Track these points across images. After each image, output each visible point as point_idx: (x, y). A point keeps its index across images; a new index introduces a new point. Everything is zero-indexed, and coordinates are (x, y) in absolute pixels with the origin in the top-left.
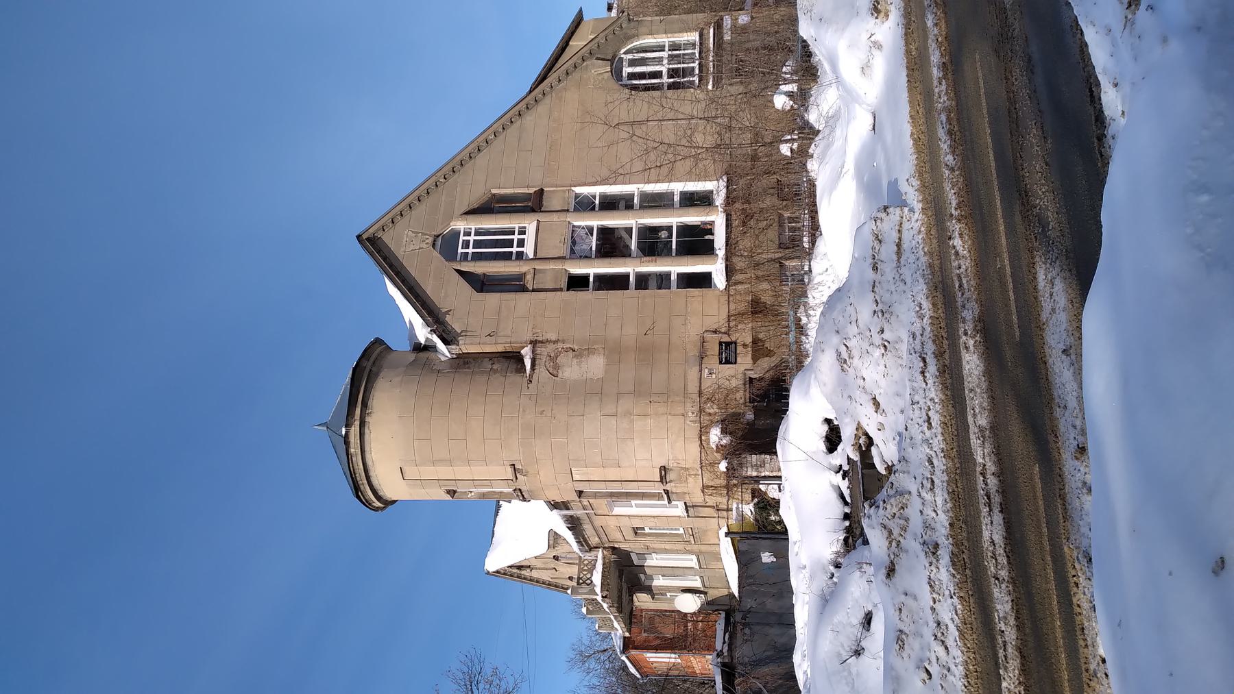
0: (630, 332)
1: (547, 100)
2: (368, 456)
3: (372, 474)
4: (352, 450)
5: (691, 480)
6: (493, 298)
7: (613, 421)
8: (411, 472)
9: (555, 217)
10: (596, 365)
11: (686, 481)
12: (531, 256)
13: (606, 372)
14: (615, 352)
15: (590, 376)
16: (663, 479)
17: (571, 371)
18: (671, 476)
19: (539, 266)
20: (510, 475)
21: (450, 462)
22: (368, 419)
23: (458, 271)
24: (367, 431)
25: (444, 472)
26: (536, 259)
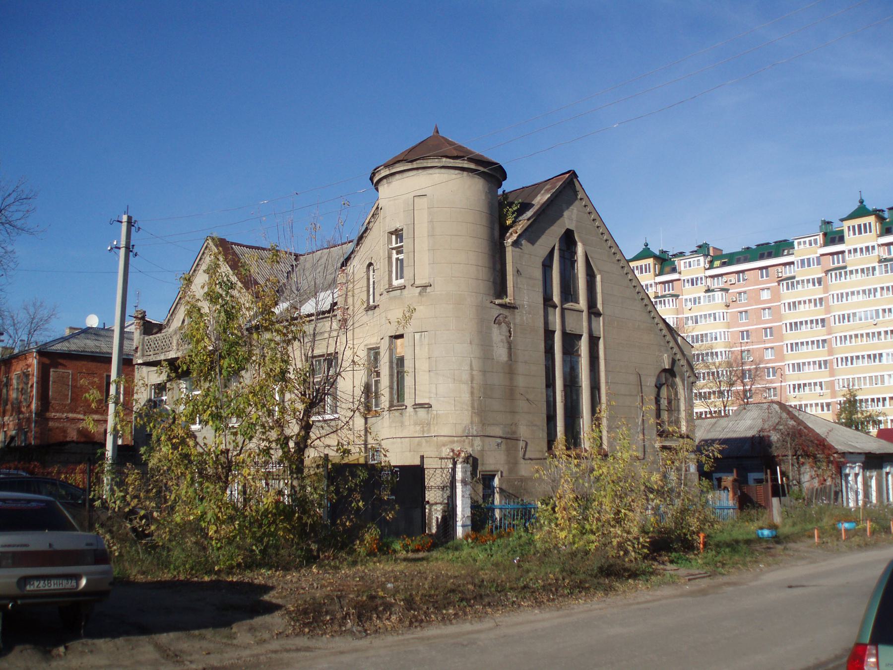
2: (437, 171)
3: (420, 171)
4: (444, 159)
5: (418, 428)
6: (538, 273)
7: (467, 368)
8: (422, 203)
9: (585, 324)
10: (501, 353)
11: (416, 424)
12: (566, 306)
14: (510, 369)
15: (495, 348)
16: (418, 406)
17: (497, 335)
18: (422, 412)
19: (558, 310)
20: (418, 282)
21: (432, 235)
22: (465, 173)
23: (553, 249)
24: (457, 172)
25: (422, 229)
26: (563, 310)
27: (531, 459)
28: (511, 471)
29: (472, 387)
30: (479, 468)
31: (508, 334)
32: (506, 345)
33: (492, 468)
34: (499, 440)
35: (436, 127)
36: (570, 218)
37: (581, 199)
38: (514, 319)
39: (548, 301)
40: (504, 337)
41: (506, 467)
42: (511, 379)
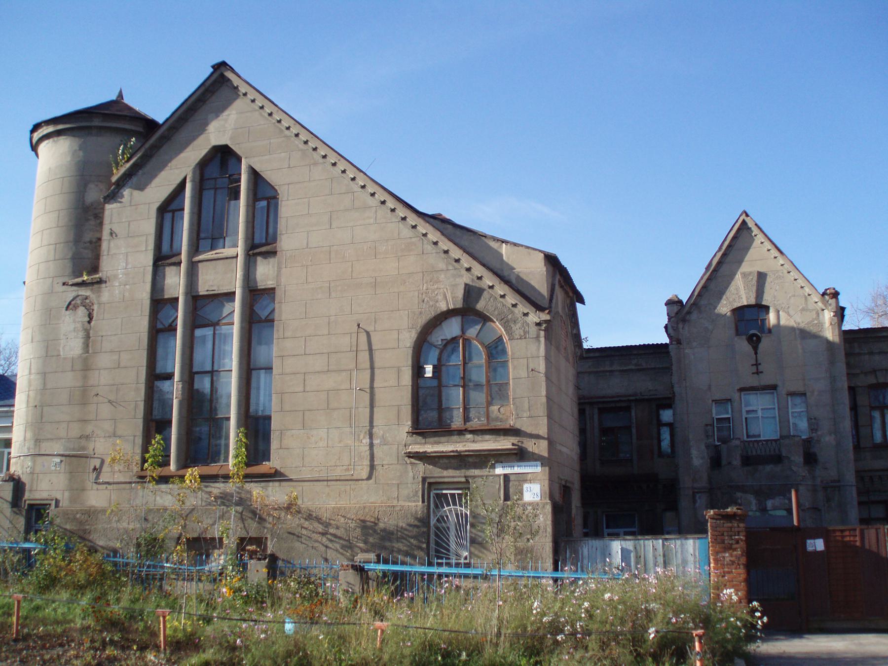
0: (102, 379)
1: (406, 232)
10: (73, 347)
13: (65, 359)
14: (85, 365)
17: (70, 325)
27: (108, 483)
28: (73, 500)
29: (28, 396)
30: (27, 495)
31: (87, 319)
32: (81, 334)
33: (45, 495)
34: (58, 460)
35: (121, 92)
36: (219, 131)
37: (245, 94)
38: (99, 296)
39: (163, 258)
40: (79, 325)
41: (67, 494)
42: (85, 377)
